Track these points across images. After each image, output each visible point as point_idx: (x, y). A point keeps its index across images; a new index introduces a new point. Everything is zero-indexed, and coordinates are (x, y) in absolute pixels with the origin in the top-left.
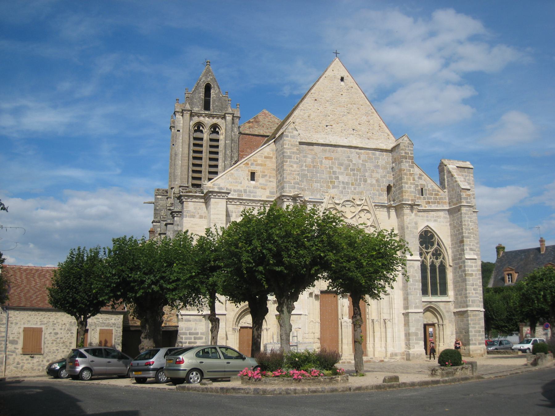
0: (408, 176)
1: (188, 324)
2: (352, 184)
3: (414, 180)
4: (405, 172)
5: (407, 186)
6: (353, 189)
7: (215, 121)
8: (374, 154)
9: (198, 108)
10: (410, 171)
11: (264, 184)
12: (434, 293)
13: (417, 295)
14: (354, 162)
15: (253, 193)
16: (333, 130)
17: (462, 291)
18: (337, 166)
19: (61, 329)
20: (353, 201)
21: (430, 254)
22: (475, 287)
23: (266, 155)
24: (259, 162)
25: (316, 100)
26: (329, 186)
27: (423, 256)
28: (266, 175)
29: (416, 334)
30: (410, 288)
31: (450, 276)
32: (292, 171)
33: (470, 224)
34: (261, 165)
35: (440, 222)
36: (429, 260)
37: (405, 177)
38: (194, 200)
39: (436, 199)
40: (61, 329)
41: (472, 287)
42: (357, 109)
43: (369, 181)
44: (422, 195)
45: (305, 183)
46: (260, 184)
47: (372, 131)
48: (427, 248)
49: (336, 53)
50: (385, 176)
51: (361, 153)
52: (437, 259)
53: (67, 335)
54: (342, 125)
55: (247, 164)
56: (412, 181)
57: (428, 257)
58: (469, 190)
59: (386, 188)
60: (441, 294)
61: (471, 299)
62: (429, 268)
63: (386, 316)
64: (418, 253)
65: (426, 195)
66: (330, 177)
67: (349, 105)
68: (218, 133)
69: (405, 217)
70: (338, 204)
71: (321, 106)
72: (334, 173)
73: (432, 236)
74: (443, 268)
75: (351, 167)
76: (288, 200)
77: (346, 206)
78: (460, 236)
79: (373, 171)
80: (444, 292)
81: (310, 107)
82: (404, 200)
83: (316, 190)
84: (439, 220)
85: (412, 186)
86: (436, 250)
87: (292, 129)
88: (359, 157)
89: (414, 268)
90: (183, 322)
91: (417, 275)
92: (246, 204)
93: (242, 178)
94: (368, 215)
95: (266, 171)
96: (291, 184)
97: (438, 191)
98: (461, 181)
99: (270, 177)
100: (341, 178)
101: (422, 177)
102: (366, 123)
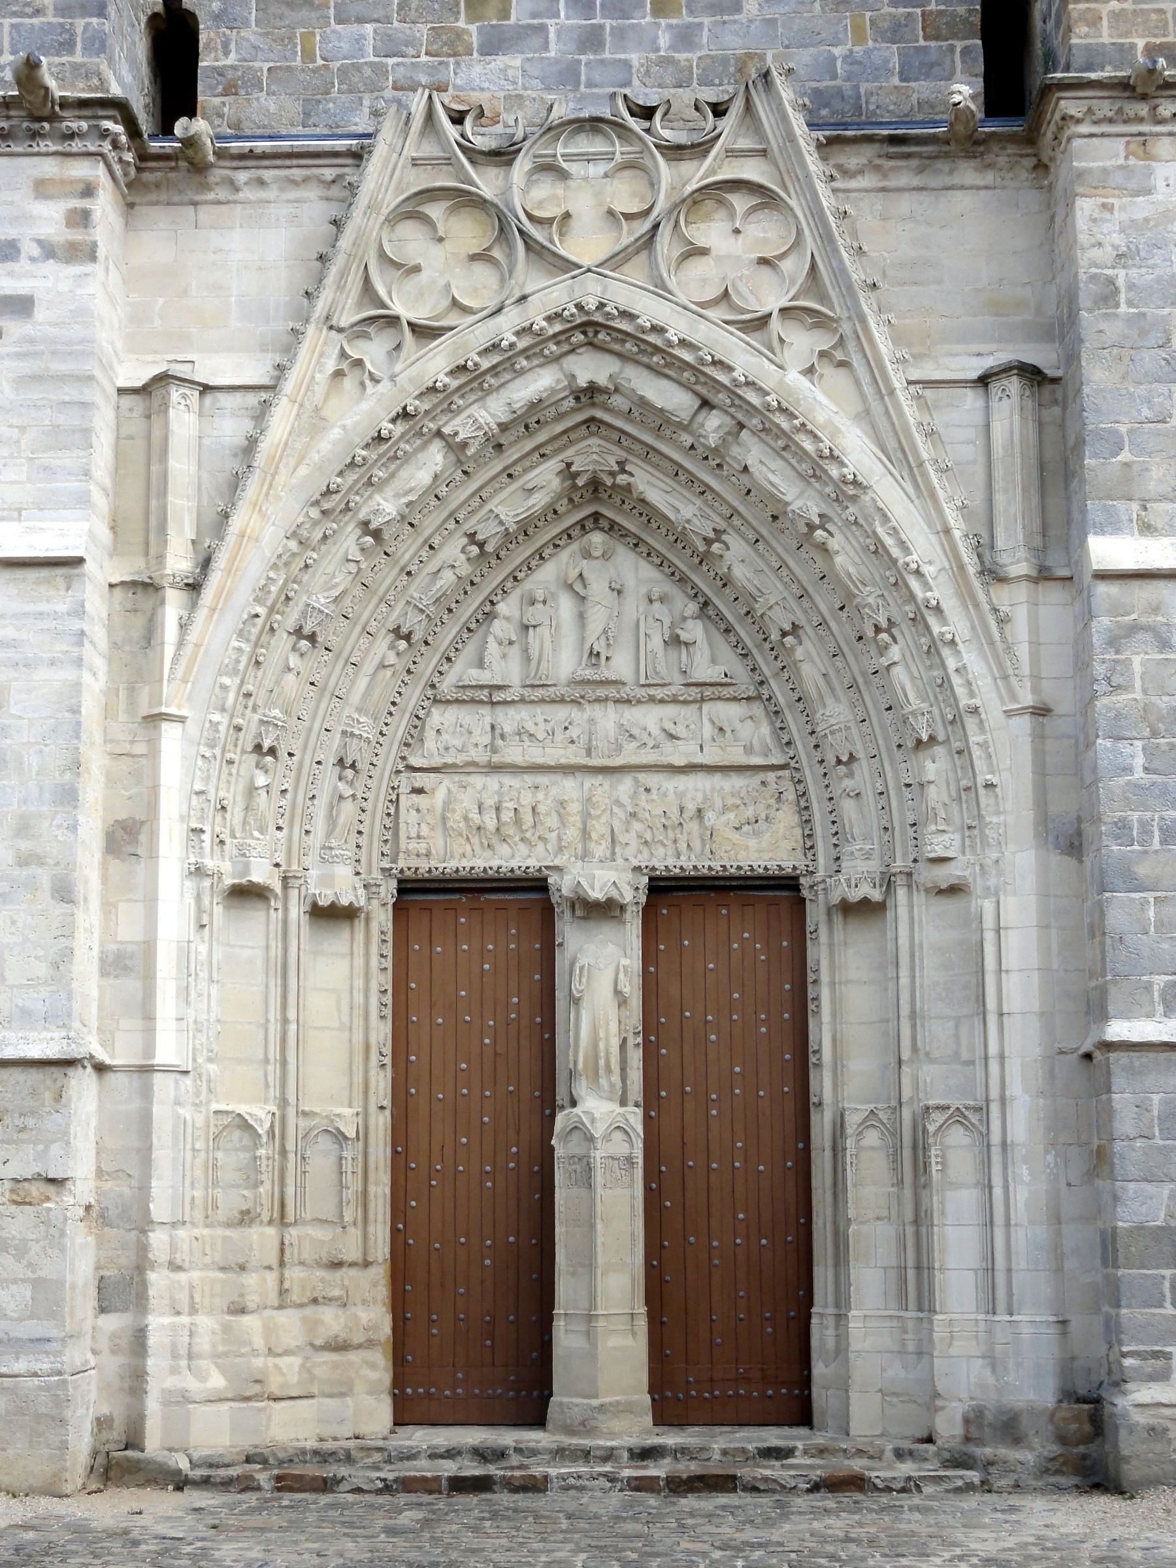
6: (664, 40)
20: (633, 123)
26: (459, 34)
30: (1123, 826)
45: (251, 33)
69: (1085, 207)
70: (503, 156)
77: (572, 168)
82: (1078, 59)
83: (343, 71)
96: (38, 12)
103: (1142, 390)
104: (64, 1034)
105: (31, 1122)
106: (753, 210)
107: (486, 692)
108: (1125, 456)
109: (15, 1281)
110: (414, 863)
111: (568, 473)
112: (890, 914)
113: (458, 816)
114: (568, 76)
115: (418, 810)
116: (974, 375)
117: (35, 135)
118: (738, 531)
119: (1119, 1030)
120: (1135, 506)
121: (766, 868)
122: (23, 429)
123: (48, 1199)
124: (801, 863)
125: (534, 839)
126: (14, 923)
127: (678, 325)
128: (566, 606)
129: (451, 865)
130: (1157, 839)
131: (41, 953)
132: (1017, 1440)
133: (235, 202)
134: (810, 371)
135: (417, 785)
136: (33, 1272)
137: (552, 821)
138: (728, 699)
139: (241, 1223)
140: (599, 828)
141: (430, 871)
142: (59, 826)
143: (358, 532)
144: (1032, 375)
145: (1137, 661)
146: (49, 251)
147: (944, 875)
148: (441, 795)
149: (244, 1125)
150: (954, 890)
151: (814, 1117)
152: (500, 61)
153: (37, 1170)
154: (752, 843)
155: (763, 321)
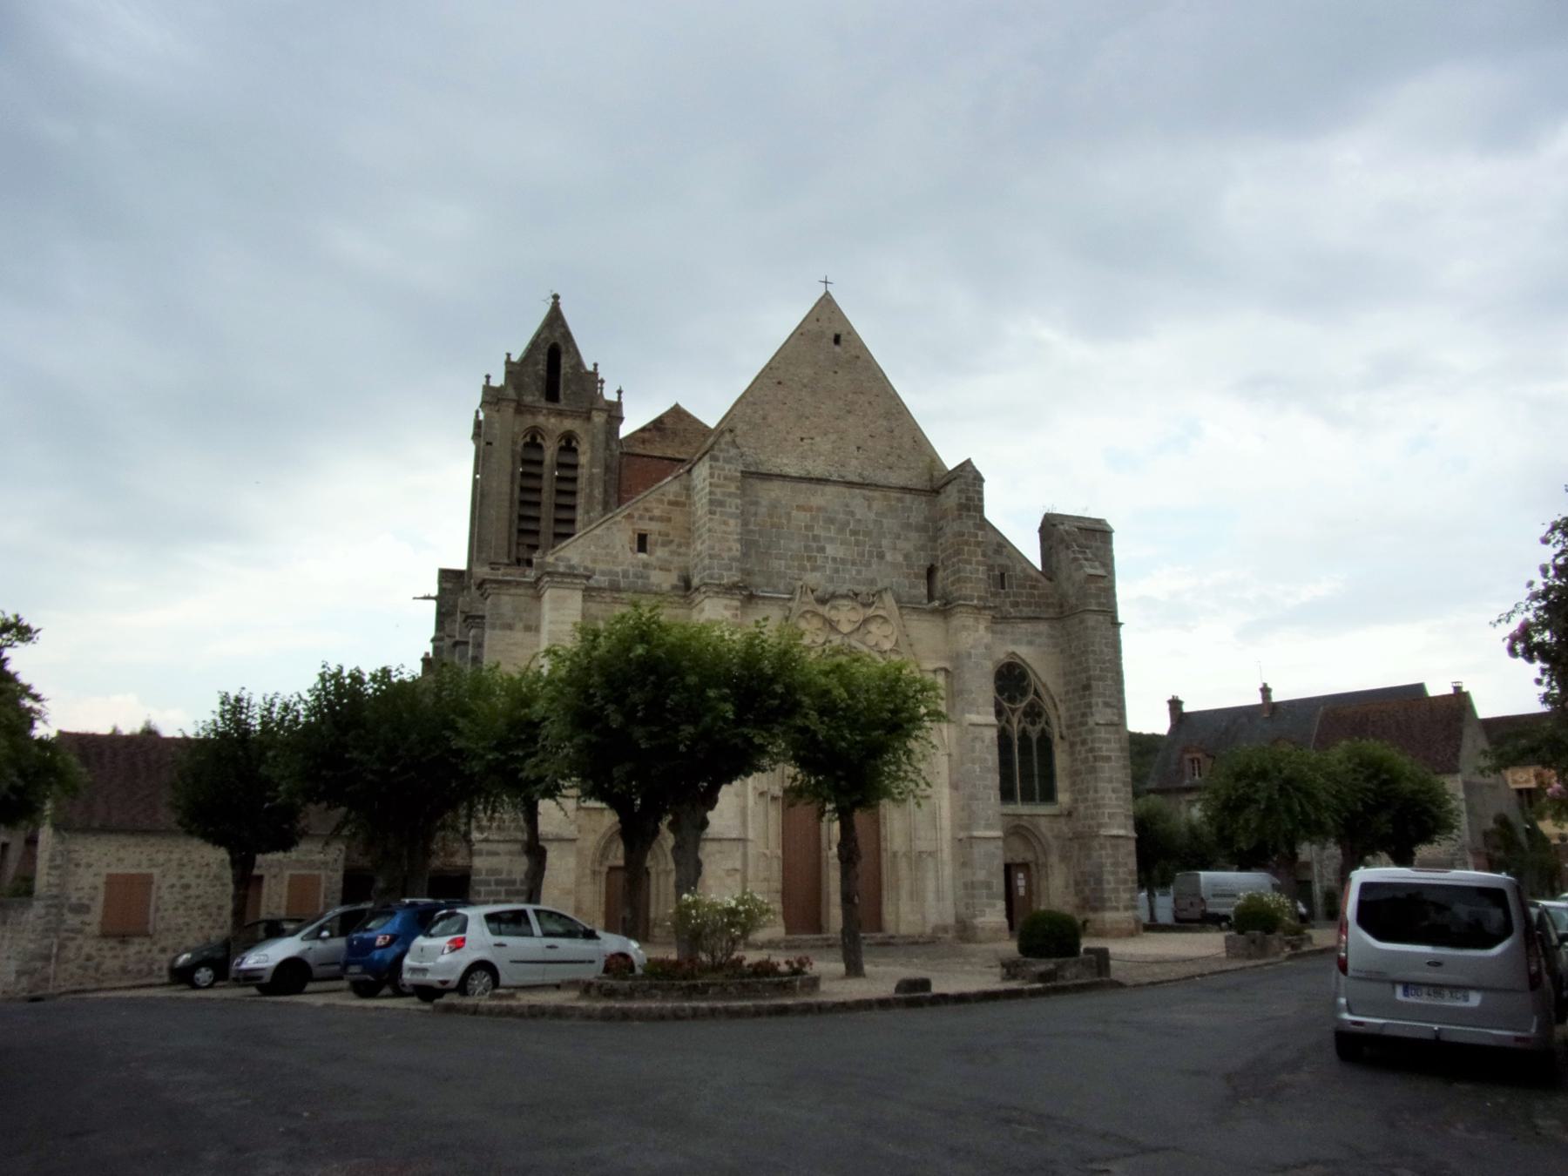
0: (972, 548)
1: (493, 862)
2: (854, 564)
3: (984, 555)
4: (966, 537)
5: (968, 567)
6: (854, 573)
7: (568, 424)
8: (900, 500)
9: (534, 395)
10: (976, 536)
12: (1028, 797)
13: (989, 799)
14: (858, 516)
15: (642, 577)
16: (814, 448)
17: (1088, 792)
18: (821, 523)
19: (198, 877)
21: (1019, 713)
22: (1115, 785)
23: (671, 497)
24: (657, 513)
25: (779, 383)
27: (1004, 718)
28: (672, 541)
29: (988, 886)
31: (1061, 760)
32: (725, 532)
33: (1106, 650)
34: (661, 519)
35: (1040, 646)
36: (1015, 726)
37: (966, 548)
38: (513, 591)
39: (1032, 596)
40: (198, 877)
41: (1109, 786)
42: (866, 405)
43: (889, 557)
44: (1003, 588)
46: (658, 559)
47: (899, 451)
48: (1011, 699)
49: (826, 282)
50: (923, 548)
51: (874, 499)
52: (1033, 723)
53: (211, 890)
55: (630, 516)
56: (980, 558)
57: (1015, 721)
58: (1104, 577)
59: (924, 572)
60: (1041, 800)
61: (1107, 811)
62: (1016, 742)
63: (922, 845)
64: (992, 710)
65: (1011, 587)
66: (807, 547)
67: (850, 396)
68: (575, 450)
72: (816, 538)
73: (1023, 676)
74: (1045, 743)
75: (851, 527)
76: (717, 593)
78: (1084, 676)
79: (898, 537)
80: (1049, 795)
81: (766, 399)
84: (1038, 641)
85: (981, 568)
86: (1031, 705)
87: (727, 443)
88: (869, 507)
89: (983, 742)
90: (482, 858)
91: (989, 757)
93: (619, 547)
94: (887, 629)
95: (671, 532)
96: (723, 559)
97: (1037, 580)
98: (1086, 559)
100: (830, 550)
101: (1004, 550)
102: (885, 433)
106: (883, 623)
108: (974, 695)
112: (908, 803)
114: (831, 580)
117: (725, 593)
119: (976, 834)
132: (947, 932)
144: (946, 670)
149: (765, 855)
151: (884, 854)
152: (814, 574)
155: (885, 652)
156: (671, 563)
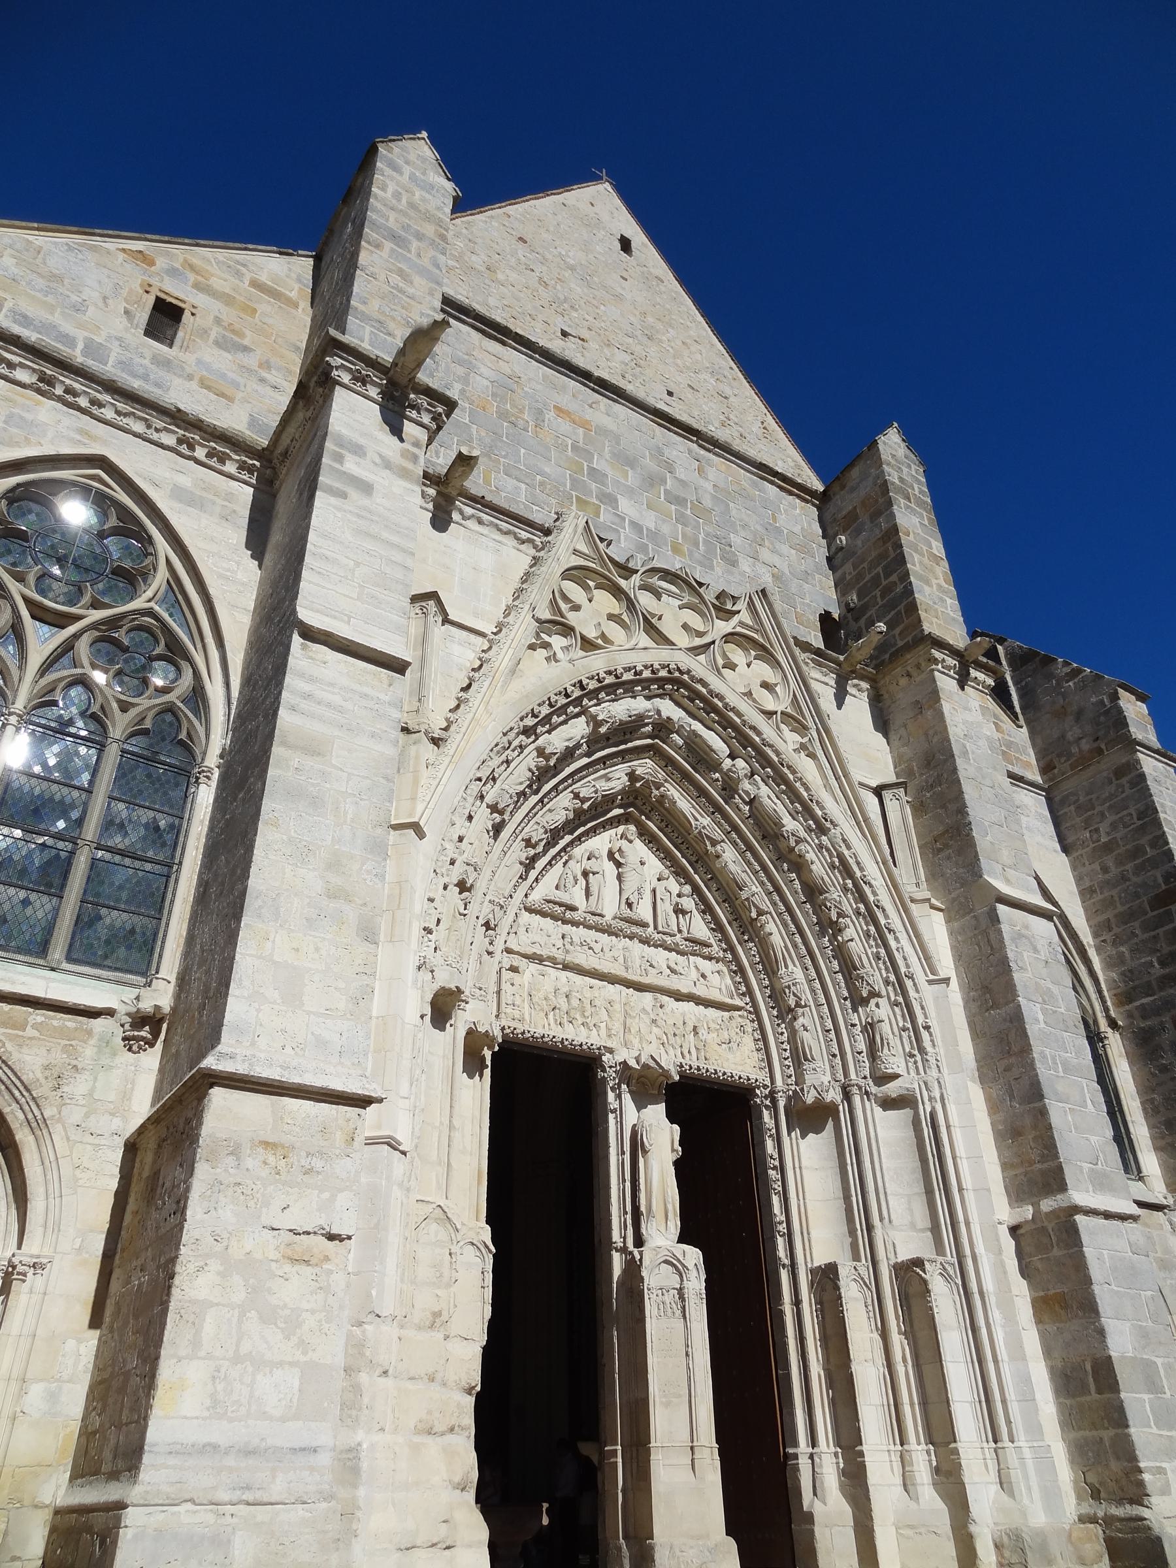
0: (926, 560)
4: (911, 538)
8: (754, 484)
11: (223, 376)
23: (264, 278)
34: (228, 300)
37: (916, 557)
46: (199, 362)
51: (708, 462)
54: (627, 358)
67: (650, 320)
71: (545, 268)
89: (1036, 950)
91: (1055, 990)
92: (83, 402)
94: (763, 671)
95: (248, 333)
99: (266, 365)
103: (989, 806)
104: (360, 1072)
105: (317, 1163)
107: (563, 909)
109: (281, 1364)
110: (513, 1024)
111: (632, 776)
113: (541, 995)
115: (512, 985)
116: (874, 784)
118: (735, 844)
120: (1000, 867)
121: (740, 1078)
122: (357, 564)
123: (327, 1259)
124: (762, 1077)
125: (591, 1025)
126: (317, 949)
127: (733, 700)
128: (609, 868)
129: (539, 1032)
130: (1060, 1069)
131: (342, 985)
133: (461, 525)
134: (794, 750)
135: (515, 964)
136: (305, 1353)
137: (604, 1015)
138: (705, 958)
139: (432, 1326)
140: (634, 1025)
141: (523, 1033)
142: (369, 872)
143: (535, 753)
145: (1025, 954)
146: (387, 465)
147: (892, 1089)
148: (527, 975)
150: (903, 1102)
153: (322, 1222)
154: (730, 1056)
156: (237, 386)
